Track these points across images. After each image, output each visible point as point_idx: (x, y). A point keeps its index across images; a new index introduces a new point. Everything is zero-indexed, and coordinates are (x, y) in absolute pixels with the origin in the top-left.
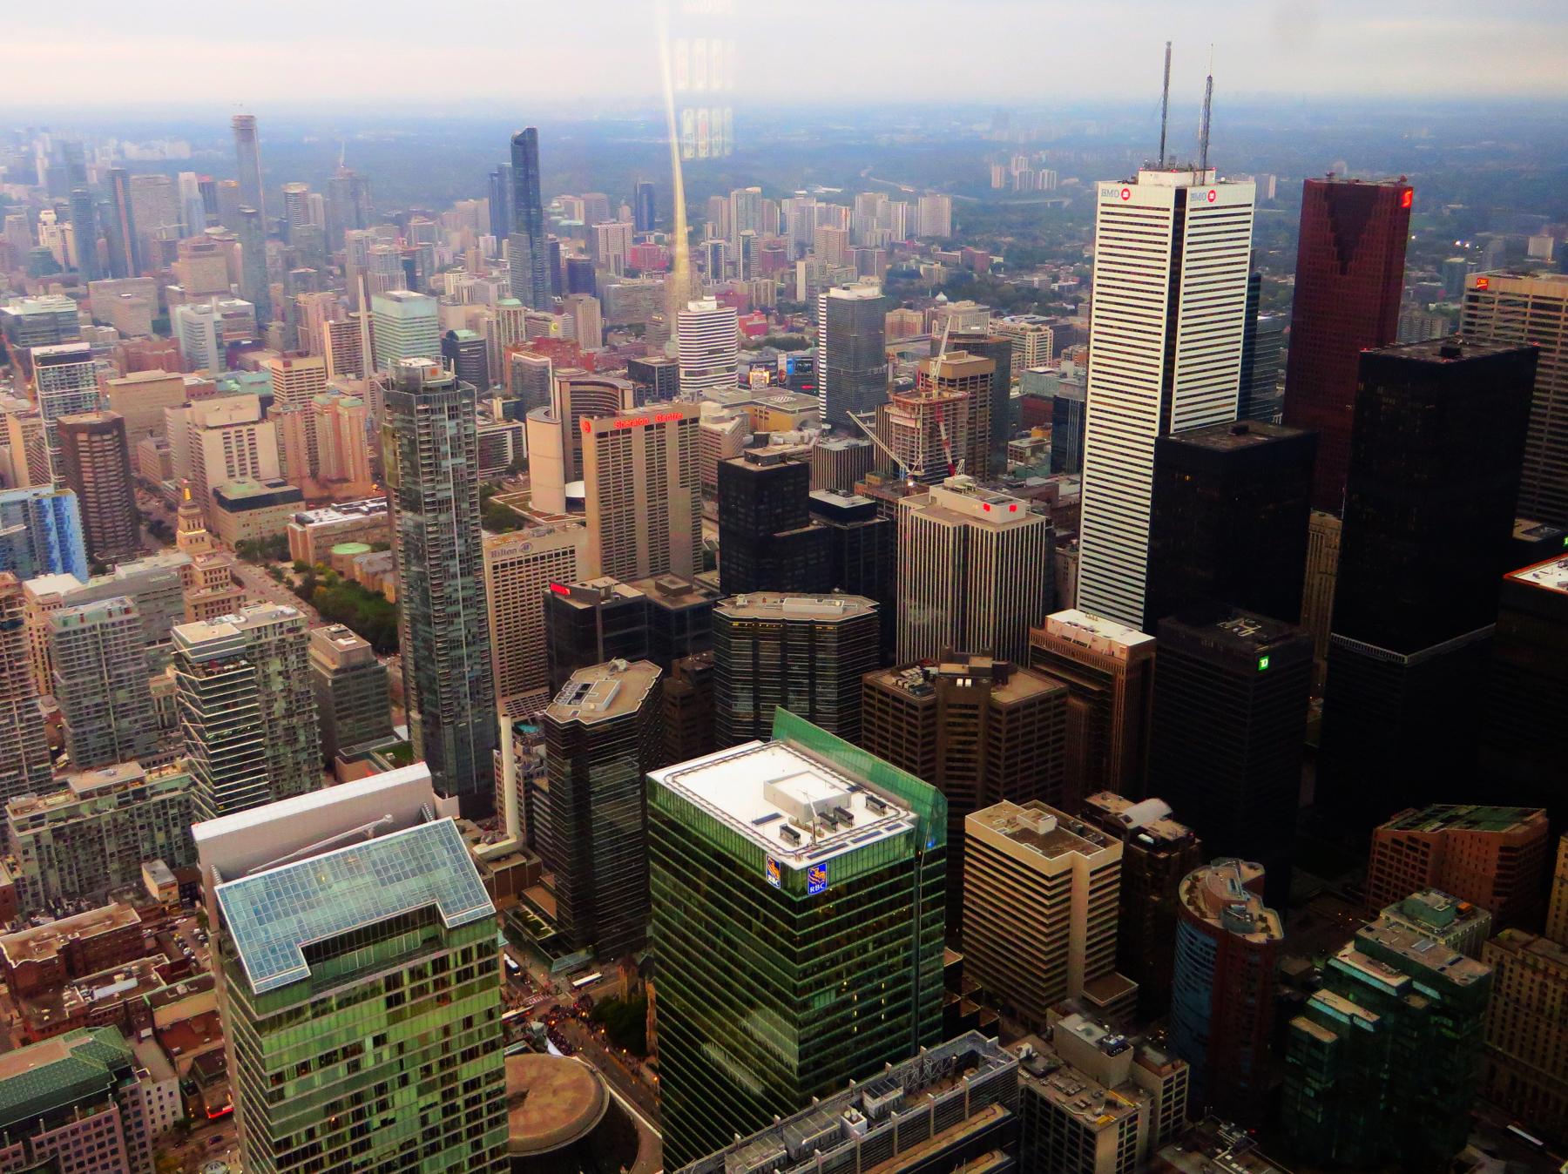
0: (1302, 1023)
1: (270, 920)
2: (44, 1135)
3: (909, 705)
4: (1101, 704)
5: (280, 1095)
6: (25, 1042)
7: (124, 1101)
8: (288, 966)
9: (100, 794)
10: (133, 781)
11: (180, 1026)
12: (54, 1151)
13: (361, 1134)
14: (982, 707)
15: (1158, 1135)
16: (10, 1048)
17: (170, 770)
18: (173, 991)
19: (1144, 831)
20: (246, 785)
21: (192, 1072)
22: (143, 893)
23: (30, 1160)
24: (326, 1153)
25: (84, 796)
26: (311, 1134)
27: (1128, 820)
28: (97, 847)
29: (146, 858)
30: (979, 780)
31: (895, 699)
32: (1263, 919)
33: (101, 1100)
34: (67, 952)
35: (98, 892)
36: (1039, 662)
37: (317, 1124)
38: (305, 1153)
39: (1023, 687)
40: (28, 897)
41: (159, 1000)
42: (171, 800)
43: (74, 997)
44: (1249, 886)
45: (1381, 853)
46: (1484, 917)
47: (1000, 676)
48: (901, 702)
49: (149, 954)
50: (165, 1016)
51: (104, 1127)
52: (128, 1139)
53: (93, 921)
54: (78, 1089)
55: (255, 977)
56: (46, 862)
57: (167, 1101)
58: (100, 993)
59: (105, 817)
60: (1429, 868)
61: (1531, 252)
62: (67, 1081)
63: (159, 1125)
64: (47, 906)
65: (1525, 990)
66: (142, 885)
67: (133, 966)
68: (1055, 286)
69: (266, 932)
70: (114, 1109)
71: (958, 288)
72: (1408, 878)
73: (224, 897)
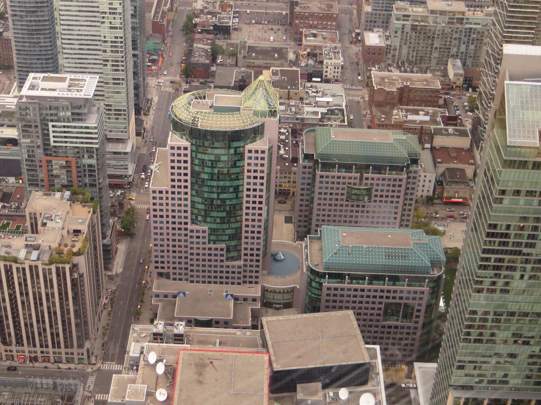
1: (527, 109)
2: (370, 175)
5: (501, 201)
6: (369, 127)
7: (410, 175)
8: (529, 137)
9: (441, 14)
10: (459, 12)
11: (444, 149)
12: (372, 184)
13: (533, 239)
16: (362, 127)
17: (479, 13)
18: (447, 130)
20: (521, 33)
21: (443, 174)
22: (445, 74)
23: (360, 184)
24: (511, 240)
25: (432, 12)
26: (508, 227)
28: (430, 42)
29: (453, 56)
33: (400, 169)
34: (402, 90)
35: (424, 66)
37: (513, 224)
38: (502, 235)
40: (390, 56)
41: (438, 132)
42: (475, 29)
43: (398, 114)
49: (439, 107)
50: (439, 141)
51: (397, 183)
52: (406, 194)
53: (419, 80)
54: (391, 159)
55: (510, 136)
56: (404, 41)
57: (427, 184)
58: (411, 117)
59: (439, 27)
62: (389, 154)
63: (420, 193)
64: (398, 63)
66: (446, 70)
67: (431, 110)
69: (523, 115)
70: (404, 176)
73: (508, 88)
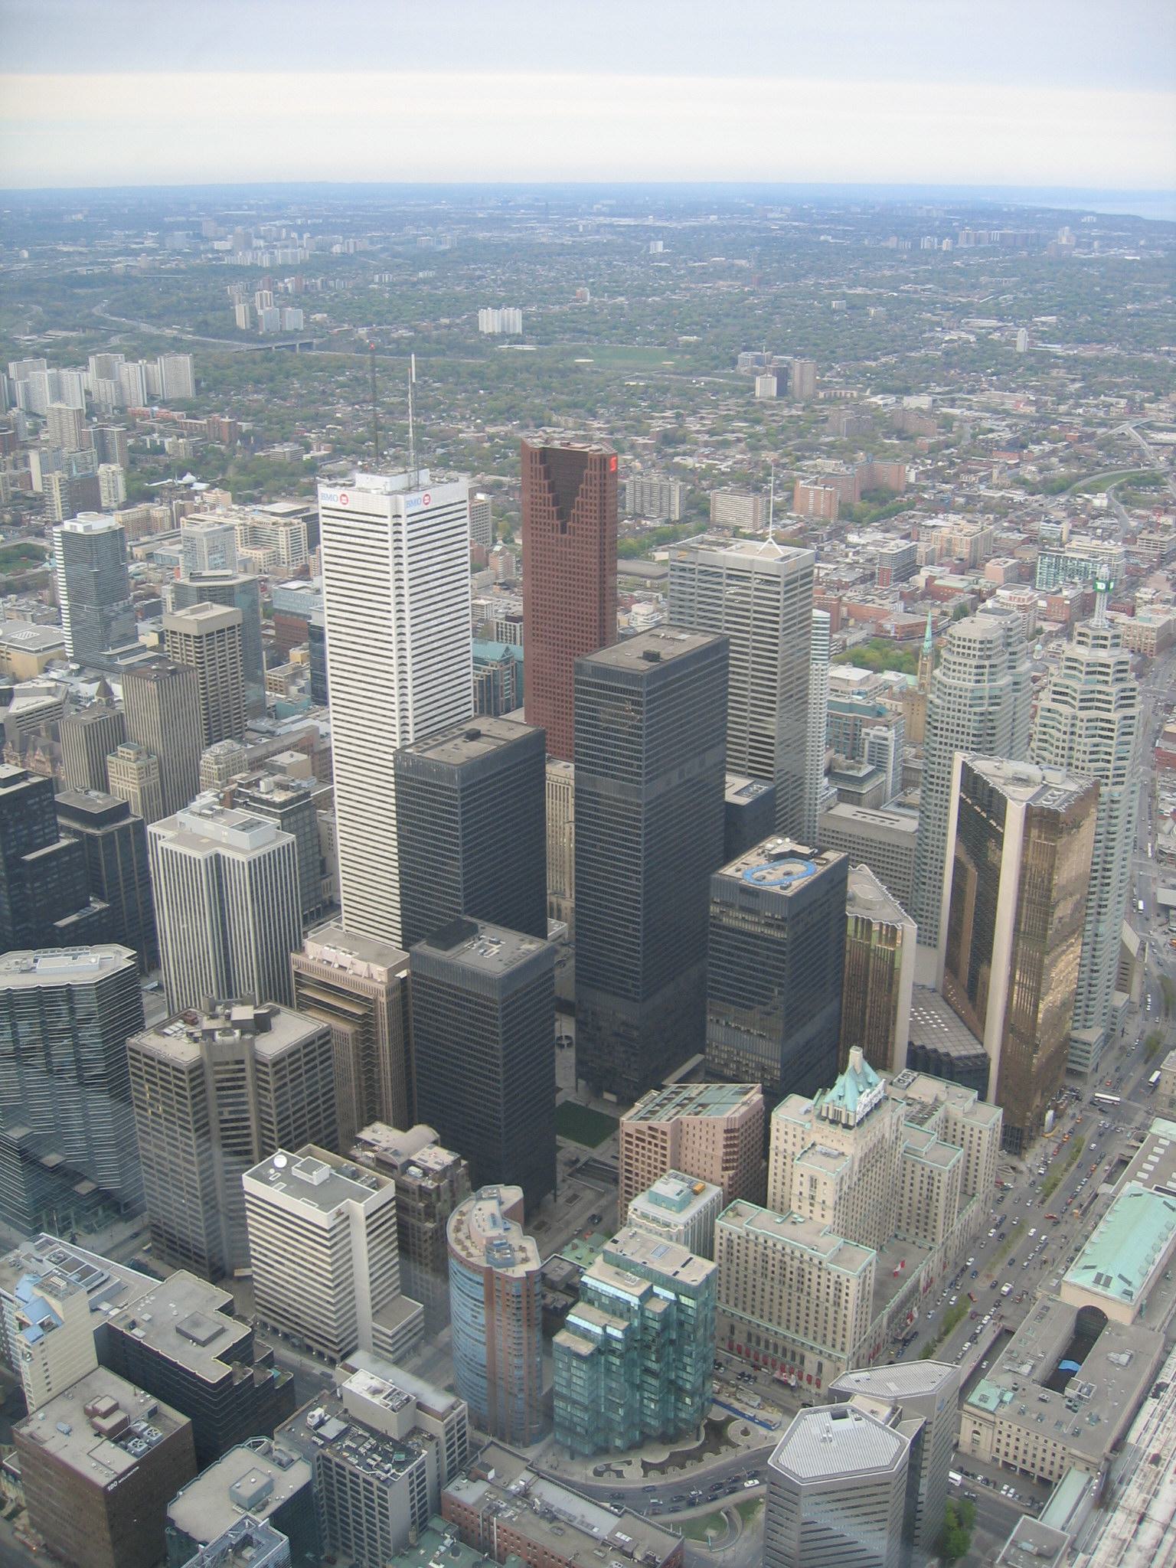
0: (561, 1338)
3: (174, 1069)
4: (366, 1024)
14: (248, 1062)
15: (446, 1469)
19: (412, 1163)
27: (396, 1153)
30: (254, 1130)
31: (160, 1062)
32: (522, 1249)
36: (304, 986)
39: (291, 1030)
44: (509, 1214)
45: (628, 1142)
46: (714, 1191)
47: (261, 1025)
48: (166, 1065)
60: (668, 1153)
61: (758, 394)
65: (751, 1261)
68: (306, 457)
71: (203, 464)
72: (652, 1162)
